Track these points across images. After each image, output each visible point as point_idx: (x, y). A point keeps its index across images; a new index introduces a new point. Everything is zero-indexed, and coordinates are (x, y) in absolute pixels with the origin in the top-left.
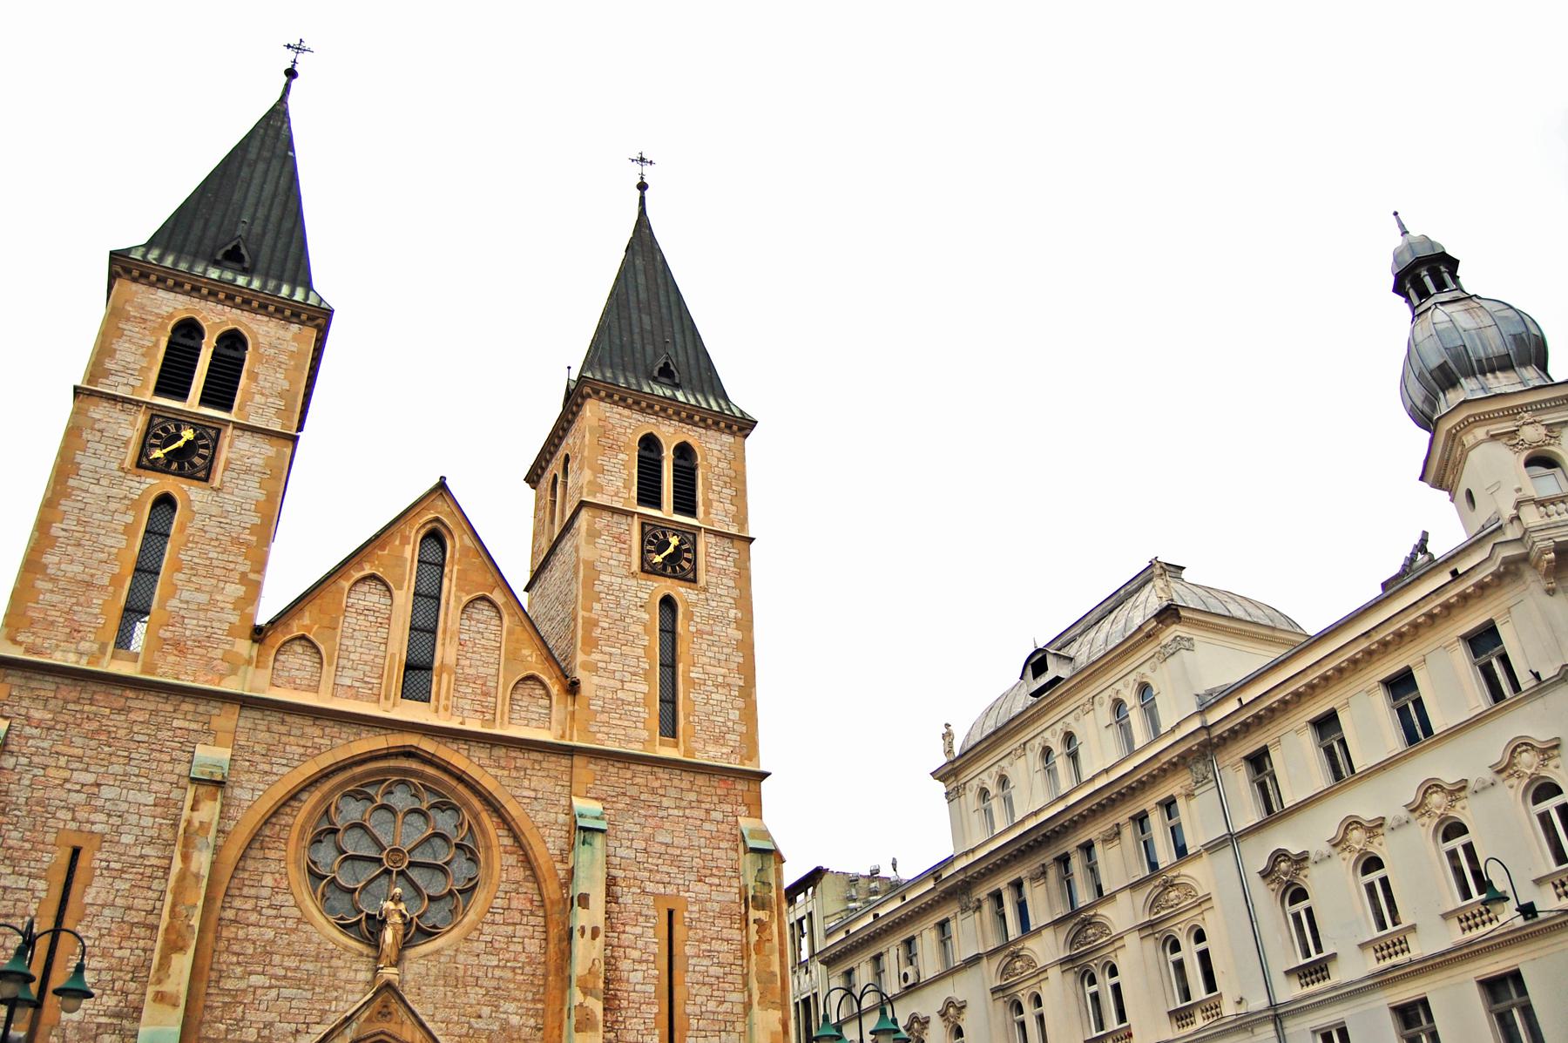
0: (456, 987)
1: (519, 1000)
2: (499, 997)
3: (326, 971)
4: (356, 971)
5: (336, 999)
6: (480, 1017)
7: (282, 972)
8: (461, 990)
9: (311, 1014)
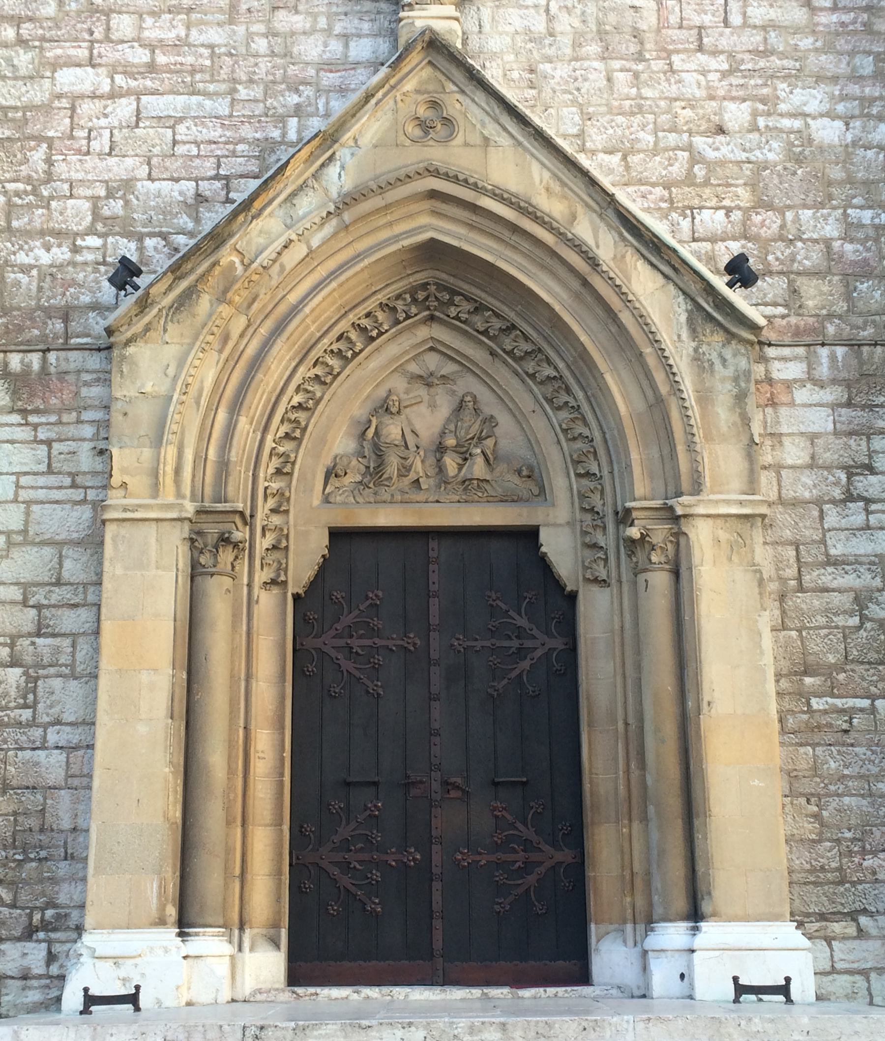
0: (640, 57)
1: (835, 79)
2: (771, 76)
3: (261, 45)
4: (346, 38)
5: (298, 111)
6: (721, 130)
7: (141, 56)
8: (659, 65)
9: (234, 154)
